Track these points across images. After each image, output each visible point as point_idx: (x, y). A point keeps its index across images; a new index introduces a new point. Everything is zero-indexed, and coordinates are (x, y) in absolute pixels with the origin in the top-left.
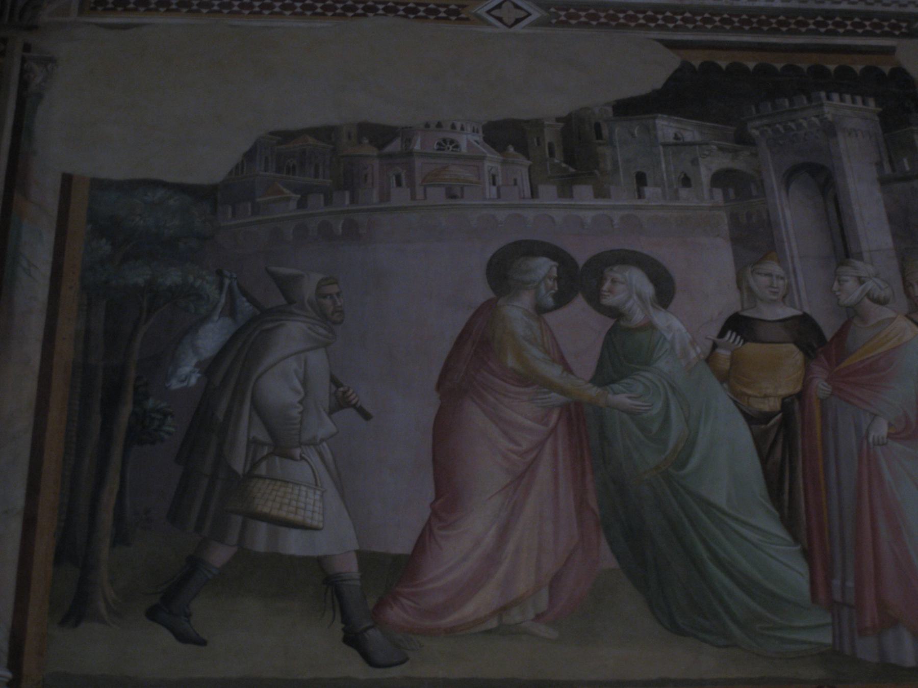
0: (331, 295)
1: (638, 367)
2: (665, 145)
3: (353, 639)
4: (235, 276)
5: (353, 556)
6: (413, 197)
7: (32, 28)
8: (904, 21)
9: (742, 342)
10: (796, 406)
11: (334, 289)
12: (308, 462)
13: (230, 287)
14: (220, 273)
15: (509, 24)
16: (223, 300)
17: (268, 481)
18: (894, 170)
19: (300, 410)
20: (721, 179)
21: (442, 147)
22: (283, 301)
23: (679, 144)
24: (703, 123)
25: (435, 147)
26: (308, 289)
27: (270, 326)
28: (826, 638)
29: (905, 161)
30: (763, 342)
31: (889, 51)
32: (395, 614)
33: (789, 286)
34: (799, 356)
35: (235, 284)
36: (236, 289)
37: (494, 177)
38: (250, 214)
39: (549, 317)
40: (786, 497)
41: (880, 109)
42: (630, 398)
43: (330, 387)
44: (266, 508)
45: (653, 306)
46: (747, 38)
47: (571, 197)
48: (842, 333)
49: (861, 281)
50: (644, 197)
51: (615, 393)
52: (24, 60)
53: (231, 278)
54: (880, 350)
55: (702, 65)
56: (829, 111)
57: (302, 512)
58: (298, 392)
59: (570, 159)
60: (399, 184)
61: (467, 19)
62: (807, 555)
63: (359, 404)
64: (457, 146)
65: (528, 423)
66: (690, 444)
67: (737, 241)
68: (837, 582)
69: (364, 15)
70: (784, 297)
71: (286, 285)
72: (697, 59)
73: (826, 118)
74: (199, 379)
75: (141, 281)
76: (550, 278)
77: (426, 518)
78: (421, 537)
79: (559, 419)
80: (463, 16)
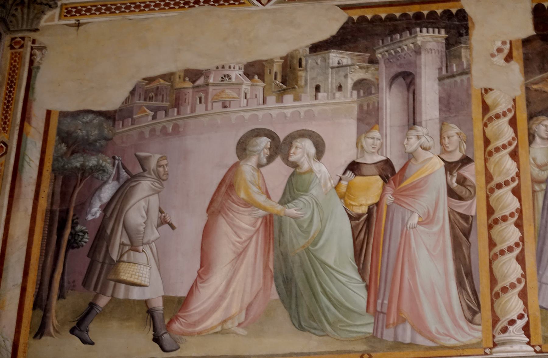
0: (163, 166)
1: (302, 193)
2: (332, 68)
3: (157, 339)
4: (121, 159)
6: (206, 109)
7: (36, 30)
9: (354, 177)
10: (375, 208)
11: (164, 162)
12: (145, 253)
13: (118, 165)
14: (114, 158)
16: (114, 172)
17: (127, 264)
18: (447, 72)
19: (144, 227)
21: (223, 80)
22: (141, 170)
23: (340, 66)
24: (354, 53)
25: (220, 79)
26: (153, 164)
29: (454, 66)
32: (176, 326)
33: (382, 144)
34: (380, 182)
36: (121, 166)
37: (246, 94)
38: (130, 124)
39: (263, 170)
40: (362, 258)
41: (447, 36)
42: (296, 210)
43: (158, 214)
44: (124, 276)
45: (313, 160)
47: (282, 102)
48: (404, 169)
49: (418, 137)
50: (318, 100)
51: (289, 208)
52: (32, 48)
53: (119, 160)
55: (358, 19)
56: (419, 40)
58: (143, 217)
60: (200, 102)
61: (244, 3)
62: (368, 288)
63: (171, 222)
64: (230, 79)
66: (321, 233)
67: (360, 120)
68: (380, 301)
69: (193, 6)
70: (379, 150)
71: (142, 162)
72: (355, 15)
73: (418, 44)
74: (101, 214)
75: (78, 165)
76: (266, 148)
77: (195, 278)
78: (192, 288)
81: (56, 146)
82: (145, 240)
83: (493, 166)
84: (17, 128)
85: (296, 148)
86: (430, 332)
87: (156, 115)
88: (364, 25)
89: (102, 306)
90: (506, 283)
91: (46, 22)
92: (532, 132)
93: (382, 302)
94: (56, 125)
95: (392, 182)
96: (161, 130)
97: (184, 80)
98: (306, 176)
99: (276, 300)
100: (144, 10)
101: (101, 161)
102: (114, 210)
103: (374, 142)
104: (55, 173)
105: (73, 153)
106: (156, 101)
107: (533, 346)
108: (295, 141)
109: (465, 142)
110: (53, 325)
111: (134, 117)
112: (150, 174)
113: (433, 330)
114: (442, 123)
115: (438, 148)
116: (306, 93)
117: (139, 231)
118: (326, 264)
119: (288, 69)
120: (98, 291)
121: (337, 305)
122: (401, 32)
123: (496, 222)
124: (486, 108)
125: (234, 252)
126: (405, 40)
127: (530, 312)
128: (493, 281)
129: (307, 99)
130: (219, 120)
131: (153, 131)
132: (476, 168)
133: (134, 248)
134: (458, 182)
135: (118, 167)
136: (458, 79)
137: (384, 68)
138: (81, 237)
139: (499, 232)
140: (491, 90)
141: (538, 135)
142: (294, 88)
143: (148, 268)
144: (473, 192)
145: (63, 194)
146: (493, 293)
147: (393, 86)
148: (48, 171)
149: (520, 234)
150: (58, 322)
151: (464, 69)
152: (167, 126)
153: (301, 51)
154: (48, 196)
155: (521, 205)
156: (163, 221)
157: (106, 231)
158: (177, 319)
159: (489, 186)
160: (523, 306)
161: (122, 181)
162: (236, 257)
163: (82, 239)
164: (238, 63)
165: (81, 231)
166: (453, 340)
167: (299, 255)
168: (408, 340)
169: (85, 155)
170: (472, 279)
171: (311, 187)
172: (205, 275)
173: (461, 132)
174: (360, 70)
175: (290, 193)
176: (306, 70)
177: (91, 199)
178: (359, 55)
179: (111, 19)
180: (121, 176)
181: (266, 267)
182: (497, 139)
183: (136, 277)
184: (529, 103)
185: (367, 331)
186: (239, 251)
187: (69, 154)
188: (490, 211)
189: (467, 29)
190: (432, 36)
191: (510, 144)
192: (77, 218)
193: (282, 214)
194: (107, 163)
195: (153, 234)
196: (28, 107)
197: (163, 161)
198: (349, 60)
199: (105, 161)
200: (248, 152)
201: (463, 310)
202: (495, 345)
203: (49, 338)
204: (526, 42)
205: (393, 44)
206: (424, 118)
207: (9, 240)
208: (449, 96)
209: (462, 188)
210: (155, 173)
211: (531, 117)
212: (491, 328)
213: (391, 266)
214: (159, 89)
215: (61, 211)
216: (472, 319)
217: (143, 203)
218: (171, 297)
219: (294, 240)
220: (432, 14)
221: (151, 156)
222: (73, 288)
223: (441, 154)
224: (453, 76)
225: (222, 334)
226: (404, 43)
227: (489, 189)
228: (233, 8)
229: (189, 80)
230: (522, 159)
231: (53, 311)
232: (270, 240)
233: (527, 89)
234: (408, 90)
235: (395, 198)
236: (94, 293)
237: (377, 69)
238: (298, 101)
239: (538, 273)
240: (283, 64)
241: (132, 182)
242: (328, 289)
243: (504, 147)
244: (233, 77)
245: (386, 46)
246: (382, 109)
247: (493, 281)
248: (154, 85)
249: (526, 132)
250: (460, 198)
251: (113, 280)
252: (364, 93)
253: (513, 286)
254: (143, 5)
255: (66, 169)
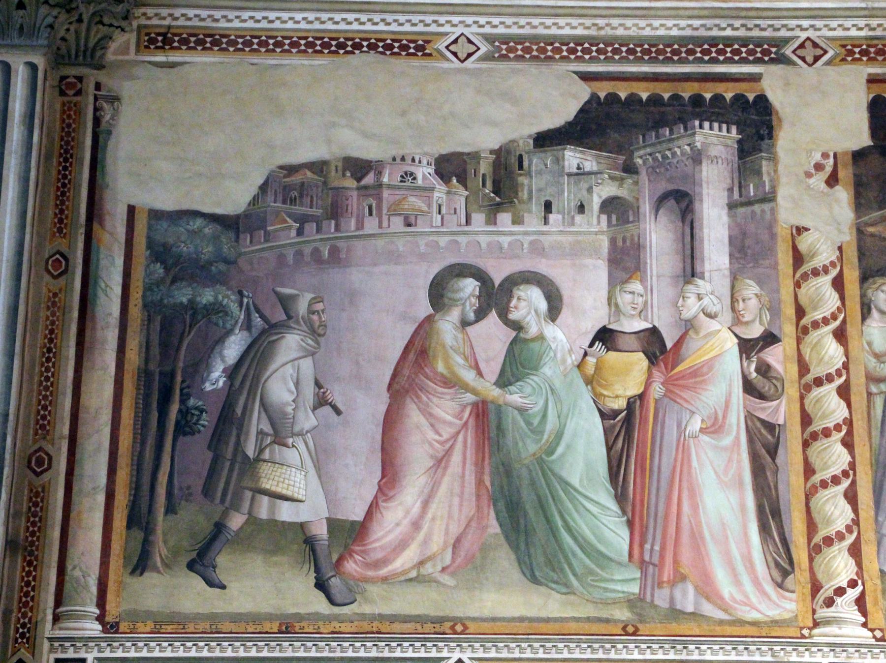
0: (318, 311)
2: (570, 175)
3: (321, 585)
5: (325, 521)
7: (101, 67)
8: (773, 46)
10: (638, 402)
11: (319, 306)
13: (248, 303)
14: (240, 293)
15: (462, 59)
16: (242, 317)
18: (741, 196)
20: (610, 205)
22: (284, 317)
23: (580, 173)
25: (399, 179)
26: (302, 307)
27: (275, 338)
28: (635, 588)
29: (751, 185)
30: (621, 351)
31: (755, 78)
32: (351, 566)
33: (646, 303)
34: (645, 363)
35: (251, 302)
37: (440, 206)
38: (262, 240)
39: (469, 329)
44: (267, 485)
46: (646, 69)
48: (678, 344)
49: (700, 297)
51: (511, 394)
52: (96, 98)
53: (248, 297)
54: (706, 358)
55: (606, 96)
56: (699, 140)
57: (291, 488)
58: (293, 393)
59: (497, 191)
60: (371, 214)
61: (430, 55)
62: (630, 524)
64: (415, 179)
65: (449, 418)
66: (559, 435)
68: (647, 546)
69: (353, 53)
70: (641, 312)
71: (286, 302)
72: (603, 90)
74: (225, 382)
75: (185, 300)
79: (470, 414)
80: (427, 51)
81: (148, 266)
82: (297, 429)
83: (809, 350)
84: (82, 230)
85: (519, 299)
86: (722, 598)
87: (303, 228)
88: (616, 108)
89: (235, 530)
90: (831, 531)
91: (115, 53)
92: (866, 301)
93: (653, 548)
94: (145, 230)
95: (662, 364)
96: (312, 254)
97: (344, 175)
98: (535, 346)
99: (497, 534)
100: (274, 51)
101: (220, 297)
102: (245, 376)
103: (634, 300)
104: (148, 311)
105: (173, 281)
106: (302, 205)
107: (872, 630)
108: (516, 288)
109: (768, 310)
110: (160, 555)
111: (269, 228)
112: (298, 323)
113: (726, 596)
114: (734, 278)
115: (727, 317)
116: (530, 212)
117: (285, 414)
118: (567, 484)
119: (503, 172)
120: (227, 504)
121: (585, 546)
122: (671, 125)
123: (814, 436)
124: (798, 259)
125: (432, 457)
126: (678, 138)
127: (866, 577)
128: (811, 527)
129: (533, 222)
130: (401, 245)
131: (299, 254)
132: (784, 349)
133: (279, 440)
134: (757, 370)
135: (248, 309)
136: (757, 208)
137: (647, 183)
138: (195, 418)
139: (819, 452)
140: (807, 230)
141: (876, 307)
142: (512, 202)
143: (303, 473)
144: (780, 389)
145: (164, 345)
146: (812, 544)
147: (661, 212)
148: (136, 305)
149: (849, 459)
150: (168, 551)
151: (765, 193)
152: (321, 249)
153: (521, 143)
154: (141, 348)
155: (850, 413)
156: (321, 401)
157: (234, 411)
158: (351, 556)
159: (803, 382)
160: (856, 569)
161: (255, 332)
162: (434, 465)
163: (198, 420)
164: (426, 154)
165: (196, 408)
166: (755, 612)
167: (528, 467)
168: (690, 609)
169: (195, 285)
170: (781, 521)
171: (542, 362)
172: (390, 489)
173: (763, 293)
174: (610, 181)
175: (511, 369)
176: (529, 174)
177: (209, 357)
178: (609, 157)
179: (221, 60)
180: (253, 324)
181: (480, 483)
182: (815, 308)
183: (285, 486)
184: (862, 254)
185: (630, 590)
186: (440, 455)
187: (168, 282)
188: (806, 419)
189: (771, 128)
190: (717, 136)
191: (834, 317)
192: (188, 387)
193: (501, 402)
194: (231, 302)
195: (307, 420)
196: (97, 197)
197: (317, 305)
198: (594, 163)
199: (228, 297)
200: (446, 301)
201: (769, 568)
202: (816, 624)
203: (155, 575)
204: (858, 156)
205: (660, 143)
206: (707, 266)
207: (82, 415)
208: (744, 234)
209: (765, 381)
210: (305, 323)
211: (865, 278)
212: (810, 598)
213: (663, 493)
214: (305, 187)
215: (161, 373)
216: (783, 581)
217: (289, 370)
218: (339, 520)
219: (520, 444)
220: (718, 98)
221: (298, 295)
222: (188, 497)
223: (732, 325)
224: (749, 203)
225: (419, 582)
226: (676, 143)
227: (804, 386)
228: (415, 62)
229: (352, 175)
230: (853, 344)
231: (159, 532)
232: (484, 440)
233: (860, 232)
234: (683, 222)
235: (667, 390)
236: (221, 508)
237: (636, 183)
238: (519, 224)
239: (876, 520)
240: (494, 162)
241: (272, 334)
242: (572, 523)
243: (826, 321)
244: (420, 177)
245: (649, 145)
246: (645, 247)
247: (811, 527)
248: (297, 178)
249: (858, 299)
250: (762, 397)
251: (251, 490)
252: (617, 220)
253: (840, 536)
254: (271, 41)
255: (165, 306)
